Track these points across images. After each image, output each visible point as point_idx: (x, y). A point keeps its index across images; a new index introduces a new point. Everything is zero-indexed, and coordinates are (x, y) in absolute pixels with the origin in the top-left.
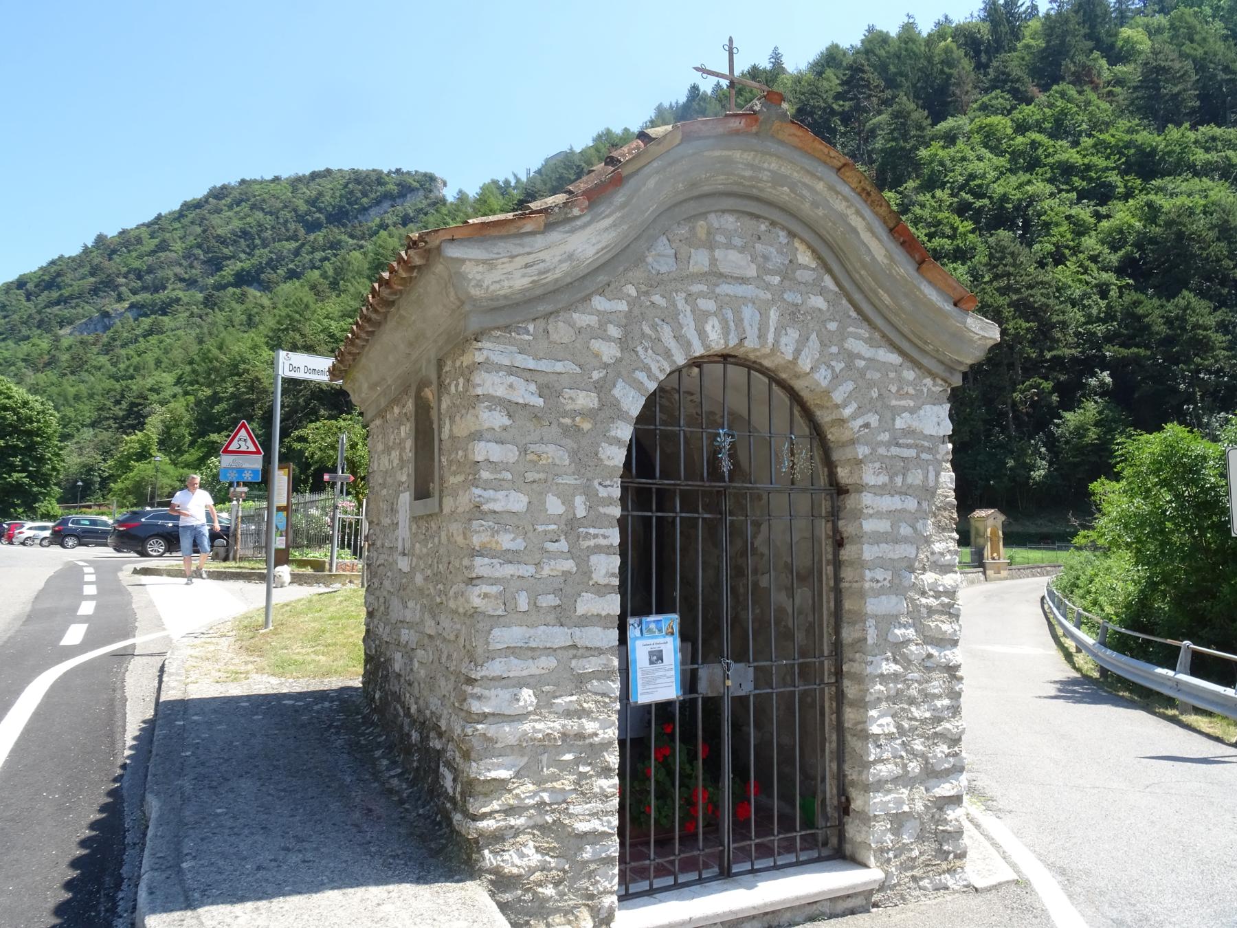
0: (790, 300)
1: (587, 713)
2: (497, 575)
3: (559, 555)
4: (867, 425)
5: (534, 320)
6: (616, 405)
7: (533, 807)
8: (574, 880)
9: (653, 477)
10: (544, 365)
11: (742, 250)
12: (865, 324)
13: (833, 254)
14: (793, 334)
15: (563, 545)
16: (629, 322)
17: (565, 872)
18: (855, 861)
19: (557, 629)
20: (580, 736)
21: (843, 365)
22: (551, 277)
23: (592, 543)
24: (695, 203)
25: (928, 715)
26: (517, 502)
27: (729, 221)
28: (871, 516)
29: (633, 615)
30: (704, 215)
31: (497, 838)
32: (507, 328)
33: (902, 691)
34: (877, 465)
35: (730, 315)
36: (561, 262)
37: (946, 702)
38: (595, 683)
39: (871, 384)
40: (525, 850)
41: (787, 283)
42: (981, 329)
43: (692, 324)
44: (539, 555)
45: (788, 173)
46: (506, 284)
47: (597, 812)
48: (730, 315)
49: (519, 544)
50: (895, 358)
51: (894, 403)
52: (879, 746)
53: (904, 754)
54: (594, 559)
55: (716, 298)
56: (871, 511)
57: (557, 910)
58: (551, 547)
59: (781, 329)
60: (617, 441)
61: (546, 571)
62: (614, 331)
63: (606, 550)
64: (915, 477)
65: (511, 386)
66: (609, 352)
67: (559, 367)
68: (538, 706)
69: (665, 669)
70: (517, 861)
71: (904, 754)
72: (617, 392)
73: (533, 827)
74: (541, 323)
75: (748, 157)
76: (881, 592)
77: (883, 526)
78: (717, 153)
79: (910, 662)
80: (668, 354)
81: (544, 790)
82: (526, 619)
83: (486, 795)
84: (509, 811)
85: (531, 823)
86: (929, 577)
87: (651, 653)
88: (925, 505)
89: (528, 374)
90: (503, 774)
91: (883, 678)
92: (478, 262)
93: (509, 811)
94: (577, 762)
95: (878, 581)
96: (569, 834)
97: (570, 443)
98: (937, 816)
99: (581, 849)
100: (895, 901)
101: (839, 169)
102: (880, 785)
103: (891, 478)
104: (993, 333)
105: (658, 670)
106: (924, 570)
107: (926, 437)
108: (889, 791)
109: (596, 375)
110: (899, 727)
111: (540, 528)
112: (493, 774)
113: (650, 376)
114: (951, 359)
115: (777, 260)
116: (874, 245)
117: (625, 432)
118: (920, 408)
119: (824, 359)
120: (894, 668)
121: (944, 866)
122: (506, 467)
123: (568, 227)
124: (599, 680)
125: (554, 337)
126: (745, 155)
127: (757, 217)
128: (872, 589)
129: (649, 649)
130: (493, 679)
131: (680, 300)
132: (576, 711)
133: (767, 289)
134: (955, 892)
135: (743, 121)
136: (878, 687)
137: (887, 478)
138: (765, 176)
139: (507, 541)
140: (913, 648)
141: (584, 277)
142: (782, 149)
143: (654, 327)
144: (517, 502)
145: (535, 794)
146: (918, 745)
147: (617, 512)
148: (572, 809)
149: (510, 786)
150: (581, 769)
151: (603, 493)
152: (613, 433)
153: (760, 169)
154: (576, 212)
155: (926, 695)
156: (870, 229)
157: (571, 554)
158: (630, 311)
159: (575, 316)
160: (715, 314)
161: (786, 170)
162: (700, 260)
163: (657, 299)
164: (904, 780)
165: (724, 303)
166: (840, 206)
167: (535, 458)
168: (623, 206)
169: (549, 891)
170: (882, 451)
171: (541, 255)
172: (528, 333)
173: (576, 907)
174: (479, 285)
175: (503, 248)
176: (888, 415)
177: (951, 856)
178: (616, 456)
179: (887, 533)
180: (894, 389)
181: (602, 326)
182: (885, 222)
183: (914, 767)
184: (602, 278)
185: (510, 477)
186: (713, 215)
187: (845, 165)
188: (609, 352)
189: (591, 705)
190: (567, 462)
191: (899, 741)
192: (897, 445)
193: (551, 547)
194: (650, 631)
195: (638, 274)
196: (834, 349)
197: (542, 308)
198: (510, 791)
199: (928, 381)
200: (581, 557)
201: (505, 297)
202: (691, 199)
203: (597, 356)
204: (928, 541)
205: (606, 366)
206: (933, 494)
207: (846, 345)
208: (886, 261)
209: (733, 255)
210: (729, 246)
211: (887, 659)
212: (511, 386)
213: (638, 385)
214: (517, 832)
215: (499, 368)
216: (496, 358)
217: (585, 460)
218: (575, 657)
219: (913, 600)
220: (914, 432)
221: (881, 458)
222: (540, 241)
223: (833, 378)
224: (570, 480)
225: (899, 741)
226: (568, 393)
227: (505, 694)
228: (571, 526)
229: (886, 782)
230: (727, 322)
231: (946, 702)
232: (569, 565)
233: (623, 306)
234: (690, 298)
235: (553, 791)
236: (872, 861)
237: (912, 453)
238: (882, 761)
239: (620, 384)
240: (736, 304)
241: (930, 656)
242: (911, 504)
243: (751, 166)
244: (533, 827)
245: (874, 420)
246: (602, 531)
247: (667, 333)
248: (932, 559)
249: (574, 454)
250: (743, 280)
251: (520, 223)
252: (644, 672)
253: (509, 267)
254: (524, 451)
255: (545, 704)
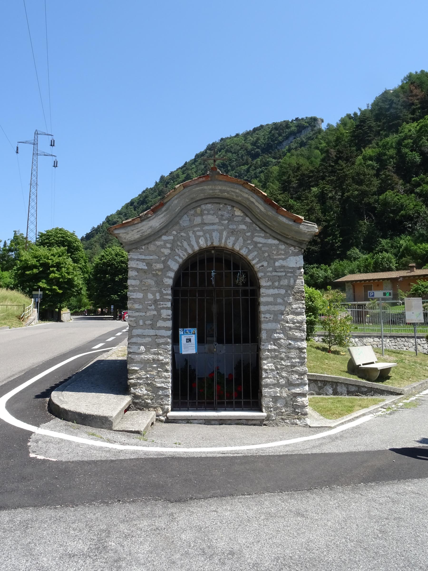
0: (231, 228)
1: (160, 354)
2: (134, 315)
3: (152, 310)
4: (262, 266)
5: (144, 245)
6: (169, 266)
7: (144, 378)
8: (156, 399)
9: (188, 286)
10: (147, 257)
11: (213, 215)
12: (262, 232)
13: (247, 210)
14: (232, 239)
15: (153, 307)
16: (173, 242)
17: (154, 397)
18: (261, 411)
19: (151, 330)
20: (158, 360)
21: (253, 246)
22: (146, 234)
23: (161, 306)
24: (194, 204)
25: (289, 364)
26: (140, 295)
27: (209, 206)
28: (264, 296)
29: (181, 328)
30: (199, 206)
31: (135, 385)
32: (136, 248)
33: (278, 355)
34: (267, 279)
35: (208, 236)
36: (148, 229)
37: (298, 360)
38: (163, 346)
39: (264, 252)
40: (142, 389)
41: (230, 222)
42: (307, 228)
43: (194, 240)
44: (146, 310)
45: (226, 189)
46: (133, 237)
47: (165, 381)
48: (208, 236)
49: (141, 307)
50: (276, 242)
51: (275, 257)
52: (267, 373)
53: (278, 376)
54: (162, 311)
55: (203, 231)
56: (265, 295)
57: (152, 407)
58: (149, 307)
59: (227, 238)
60: (169, 277)
61: (148, 314)
62: (168, 245)
63: (167, 308)
64: (285, 282)
65: (137, 264)
66: (167, 251)
67: (151, 257)
68: (146, 351)
69: (192, 344)
70: (140, 392)
71: (278, 376)
72: (169, 263)
73: (145, 384)
74: (146, 246)
75: (210, 187)
76: (269, 321)
77: (271, 299)
78: (199, 188)
79: (281, 346)
80: (186, 250)
81: (148, 374)
82: (142, 327)
83: (132, 374)
84: (138, 378)
85: (145, 382)
86: (290, 317)
87: (187, 339)
88: (289, 292)
89: (143, 260)
90: (136, 368)
91: (269, 350)
92: (123, 233)
93: (138, 378)
94: (157, 367)
95: (267, 318)
96: (155, 387)
97: (155, 279)
98: (293, 399)
99: (159, 391)
100: (273, 425)
101: (243, 185)
102: (267, 386)
103: (273, 283)
104: (315, 228)
105: (189, 344)
106: (288, 314)
107: (290, 268)
108: (271, 388)
109: (163, 259)
110: (276, 367)
111: (146, 302)
112: (133, 368)
113: (180, 257)
114: (299, 240)
115: (226, 215)
116: (260, 206)
117: (172, 274)
118: (287, 258)
119: (245, 245)
120: (274, 347)
121: (296, 417)
122: (136, 286)
123: (148, 220)
124: (164, 345)
125: (150, 249)
126: (208, 187)
127: (219, 203)
128: (265, 321)
129: (186, 338)
130: (133, 343)
131: (191, 234)
132: (157, 353)
133: (223, 226)
134: (300, 426)
135: (204, 178)
136: (267, 353)
137: (271, 283)
138: (217, 191)
139: (136, 306)
140: (282, 341)
141: (158, 231)
142: (220, 183)
143: (181, 243)
144: (140, 295)
145: (145, 375)
146: (284, 374)
147: (170, 297)
148: (156, 380)
149: (138, 372)
150: (159, 369)
151: (165, 292)
152: (167, 275)
153: (215, 189)
154: (150, 215)
155: (288, 357)
156: (257, 201)
157: (155, 310)
158: (174, 239)
159: (157, 242)
160: (202, 236)
161: (224, 188)
162: (198, 220)
163: (183, 234)
164: (278, 385)
165: (205, 232)
166: (246, 196)
167: (144, 283)
168: (165, 211)
169: (149, 401)
170: (269, 274)
171: (142, 228)
172: (143, 249)
173: (157, 407)
174: (125, 239)
175: (129, 229)
176: (272, 261)
177: (300, 414)
178: (170, 282)
179: (272, 302)
180: (275, 253)
181: (165, 244)
182: (262, 198)
183: (282, 381)
184: (164, 231)
185: (137, 289)
186: (203, 205)
187: (244, 183)
188: (167, 251)
189: (162, 352)
190: (154, 284)
191: (276, 372)
192: (276, 272)
193: (149, 307)
194: (186, 333)
195: (177, 227)
196: (249, 242)
197: (146, 242)
198: (138, 373)
199: (292, 248)
200: (158, 310)
201: (134, 240)
202: (194, 202)
203: (163, 253)
204: (290, 304)
205: (166, 256)
206: (293, 288)
207: (254, 240)
208: (265, 211)
209: (210, 217)
210: (208, 214)
211: (271, 344)
212: (137, 264)
213: (176, 261)
214: (140, 384)
215: (134, 259)
216: (133, 257)
217: (159, 283)
218: (157, 338)
219: (282, 325)
220: (284, 266)
221: (269, 277)
222: (140, 225)
223: (248, 251)
224: (154, 289)
225: (276, 372)
226: (154, 264)
227: (136, 347)
228: (155, 302)
229: (270, 385)
230: (206, 238)
231: (298, 360)
232: (155, 313)
233: (171, 238)
234: (194, 232)
235: (150, 374)
236: (264, 410)
237: (284, 274)
238: (268, 378)
239: (170, 260)
240: (210, 232)
241: (290, 344)
242: (283, 291)
243: (212, 189)
244: (145, 384)
245: (265, 264)
246: (164, 303)
247: (185, 244)
248: (293, 310)
249: (156, 282)
250: (213, 224)
251: (133, 222)
252: (184, 345)
253: (133, 233)
254: (141, 281)
255: (148, 351)
